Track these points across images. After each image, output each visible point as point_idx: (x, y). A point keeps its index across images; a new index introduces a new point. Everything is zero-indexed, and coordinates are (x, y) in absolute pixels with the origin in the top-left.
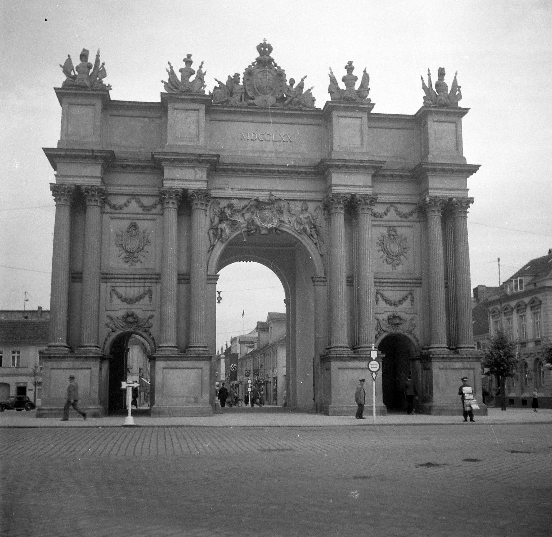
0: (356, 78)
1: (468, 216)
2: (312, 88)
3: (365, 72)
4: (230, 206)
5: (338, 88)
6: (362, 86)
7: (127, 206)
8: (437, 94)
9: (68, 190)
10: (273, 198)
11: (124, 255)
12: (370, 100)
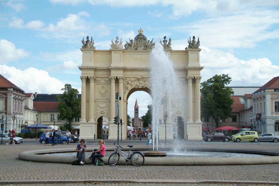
0: (166, 41)
2: (155, 42)
3: (170, 39)
4: (130, 80)
6: (169, 43)
10: (143, 78)
11: (101, 94)
12: (171, 47)
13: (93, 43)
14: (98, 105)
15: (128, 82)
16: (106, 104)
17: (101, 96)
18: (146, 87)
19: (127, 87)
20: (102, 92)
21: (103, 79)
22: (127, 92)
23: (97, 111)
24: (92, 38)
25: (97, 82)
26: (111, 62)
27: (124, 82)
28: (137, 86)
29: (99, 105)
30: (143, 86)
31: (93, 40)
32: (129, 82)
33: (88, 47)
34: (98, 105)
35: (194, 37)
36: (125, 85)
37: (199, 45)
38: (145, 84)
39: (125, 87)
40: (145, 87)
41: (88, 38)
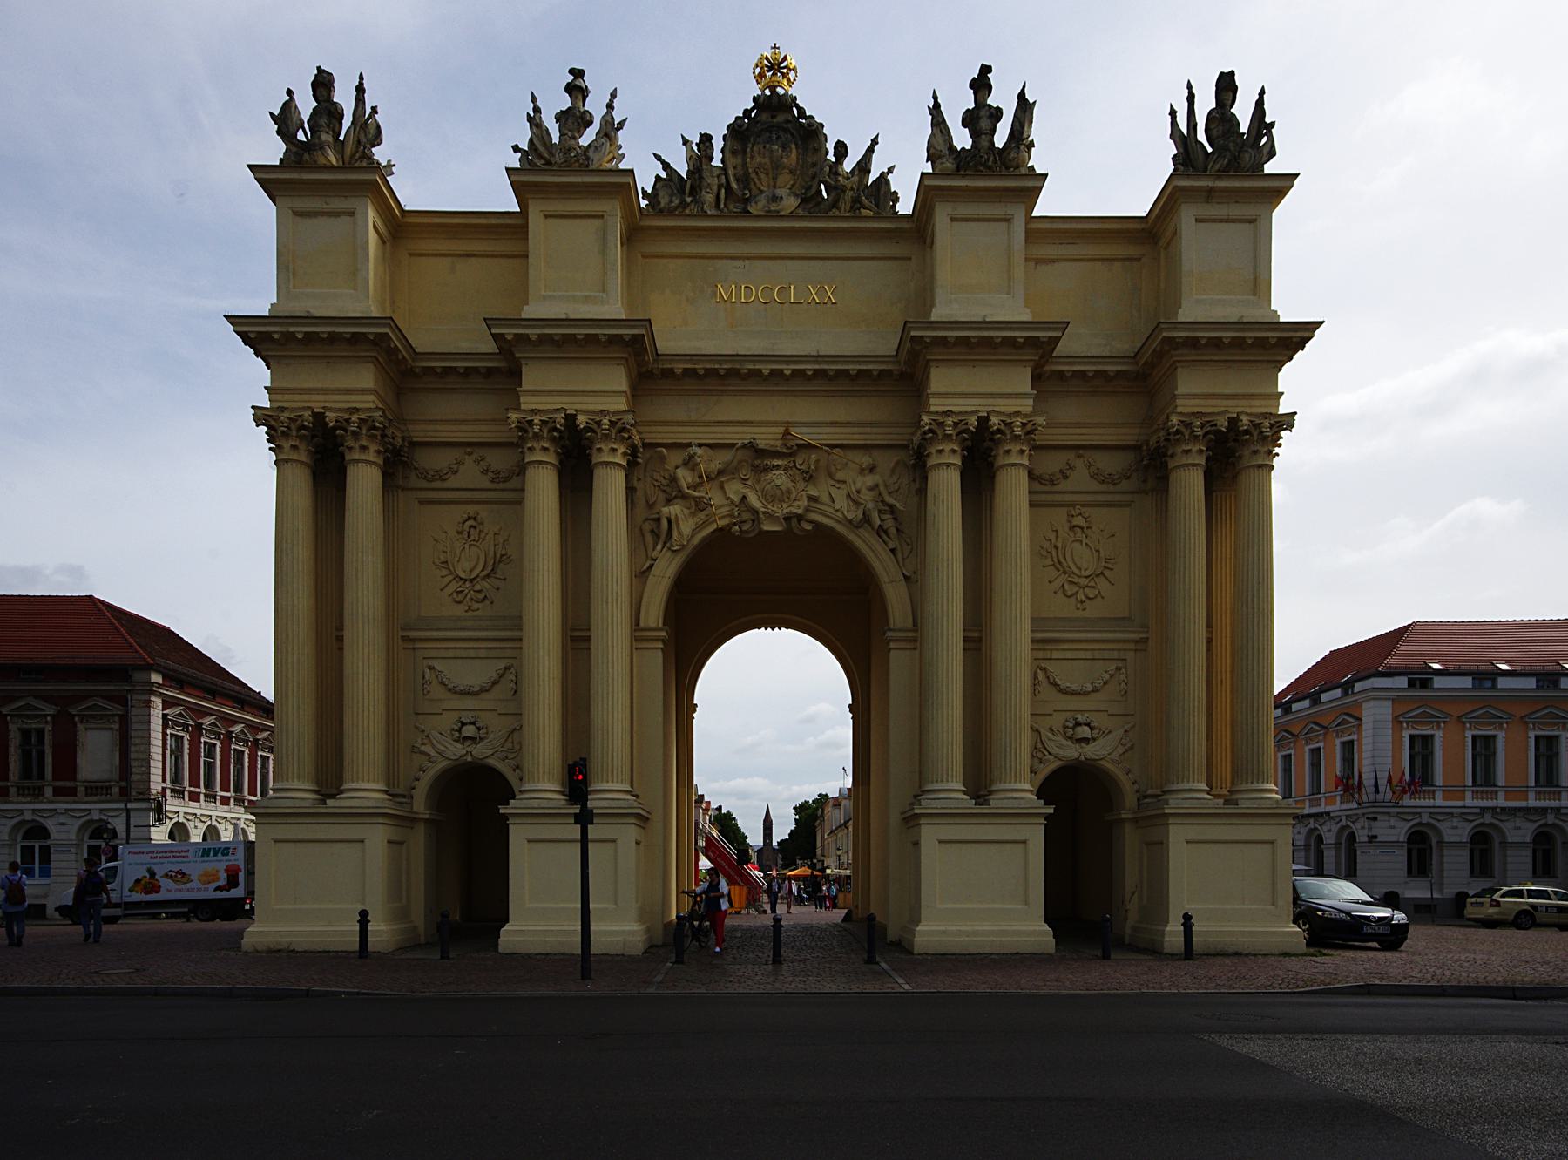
1: (1274, 464)
5: (952, 148)
8: (1210, 150)
13: (372, 131)
15: (674, 480)
16: (501, 665)
18: (817, 525)
19: (665, 523)
22: (666, 569)
24: (360, 89)
25: (425, 484)
26: (522, 292)
27: (636, 484)
28: (746, 516)
29: (438, 674)
30: (795, 510)
31: (374, 110)
32: (685, 477)
34: (428, 674)
35: (1226, 85)
36: (650, 506)
37: (1272, 154)
38: (812, 499)
39: (647, 526)
40: (808, 527)
41: (323, 84)
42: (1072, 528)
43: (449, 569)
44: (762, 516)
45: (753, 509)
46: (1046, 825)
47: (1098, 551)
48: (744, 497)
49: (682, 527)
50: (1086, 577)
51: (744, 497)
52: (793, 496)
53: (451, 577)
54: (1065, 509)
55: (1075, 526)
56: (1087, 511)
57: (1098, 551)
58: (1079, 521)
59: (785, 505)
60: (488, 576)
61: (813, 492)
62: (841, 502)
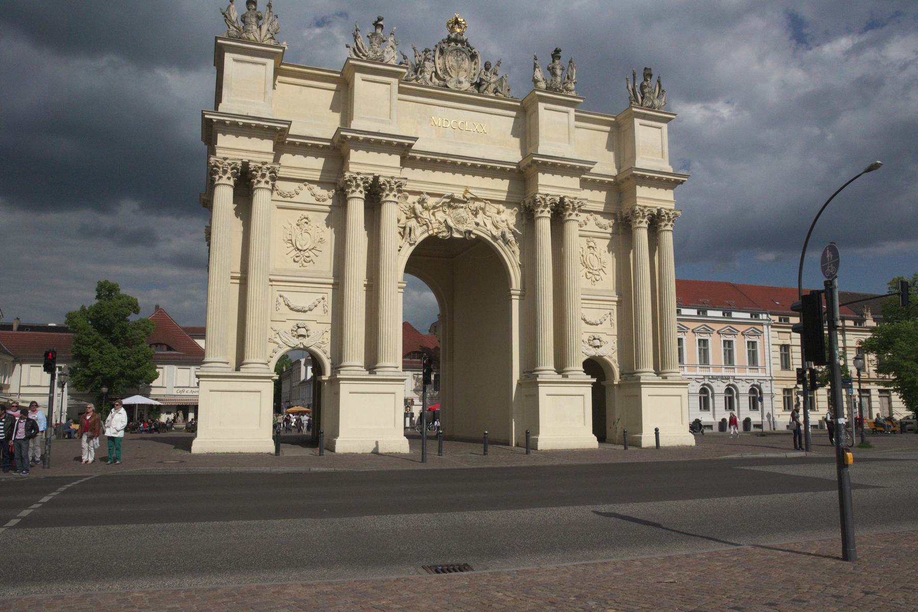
7: (298, 194)
9: (232, 166)
11: (295, 253)
14: (281, 300)
17: (297, 259)
18: (479, 239)
19: (408, 230)
20: (304, 243)
21: (305, 188)
23: (278, 326)
25: (280, 198)
33: (252, 38)
38: (477, 224)
40: (473, 236)
42: (589, 247)
43: (292, 244)
44: (454, 230)
45: (449, 226)
46: (592, 387)
47: (600, 259)
48: (446, 220)
49: (416, 233)
50: (596, 270)
51: (446, 220)
52: (468, 221)
53: (293, 248)
54: (586, 238)
55: (590, 247)
56: (596, 240)
57: (600, 259)
58: (592, 244)
59: (464, 226)
60: (313, 249)
61: (477, 220)
62: (490, 226)
